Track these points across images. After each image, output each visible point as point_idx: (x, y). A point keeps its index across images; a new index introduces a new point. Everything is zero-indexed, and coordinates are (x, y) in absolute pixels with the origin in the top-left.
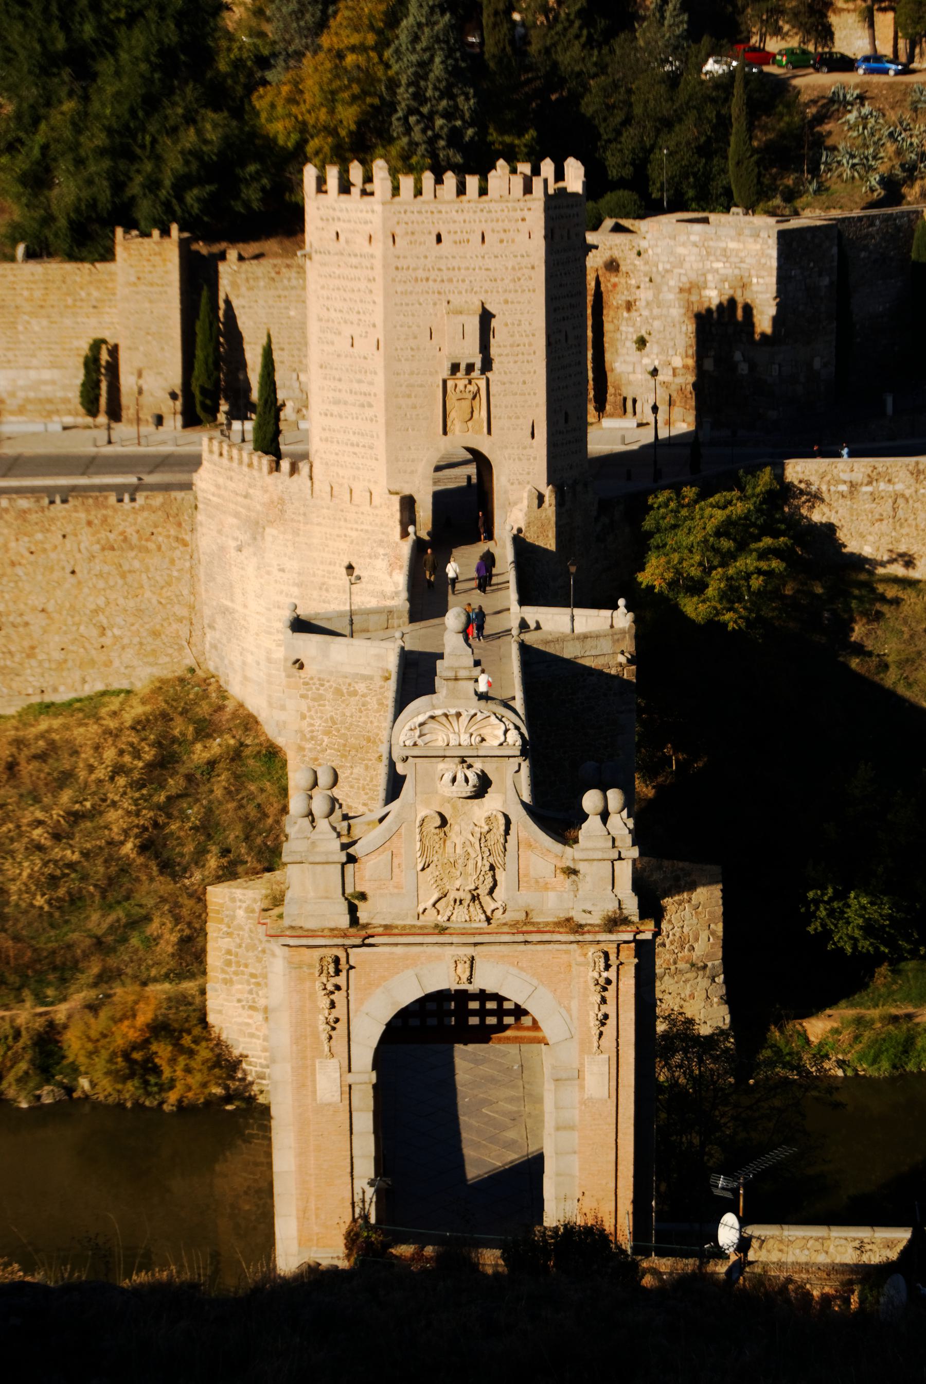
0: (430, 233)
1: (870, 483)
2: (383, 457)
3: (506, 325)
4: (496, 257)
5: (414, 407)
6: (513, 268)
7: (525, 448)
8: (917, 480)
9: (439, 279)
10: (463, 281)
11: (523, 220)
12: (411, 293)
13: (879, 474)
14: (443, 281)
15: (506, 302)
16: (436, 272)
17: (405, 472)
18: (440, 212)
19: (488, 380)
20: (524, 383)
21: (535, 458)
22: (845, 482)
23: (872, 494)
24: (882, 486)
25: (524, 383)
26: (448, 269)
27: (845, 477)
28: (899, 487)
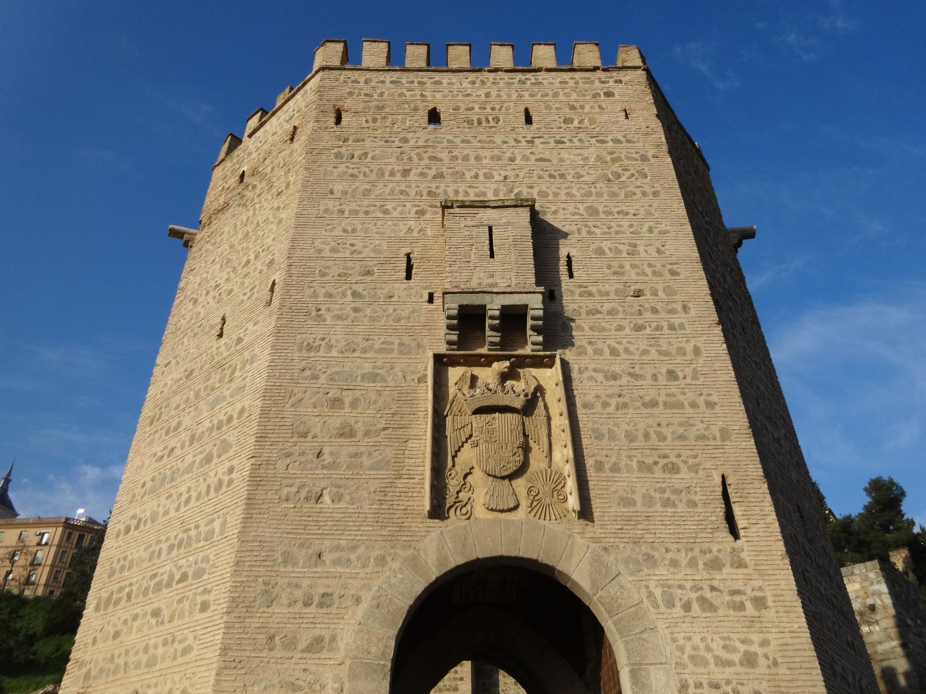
0: (416, 109)
2: (220, 596)
3: (600, 252)
5: (347, 432)
6: (599, 158)
7: (715, 565)
9: (432, 172)
10: (489, 176)
11: (608, 94)
12: (366, 193)
14: (440, 176)
15: (593, 212)
16: (426, 161)
17: (290, 644)
18: (439, 83)
19: (565, 365)
21: (760, 603)
25: (672, 375)
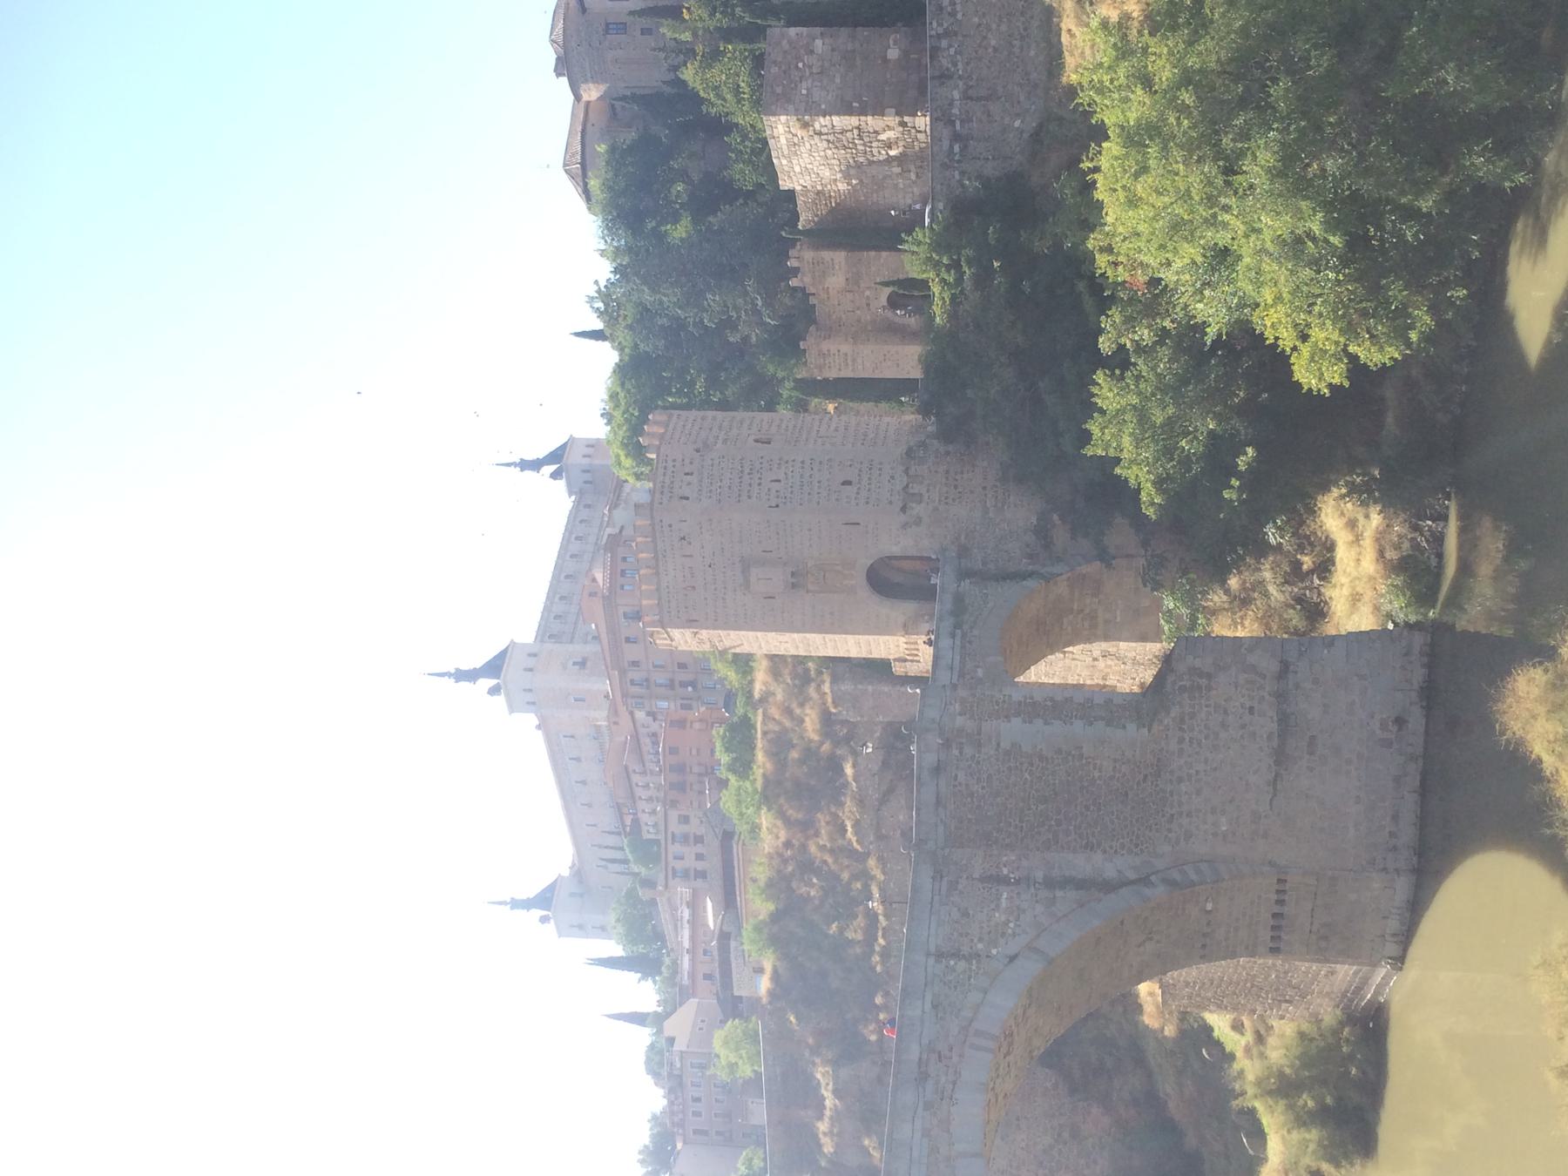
1: (952, 123)
3: (760, 542)
4: (703, 547)
5: (832, 613)
6: (712, 535)
7: (867, 532)
8: (950, 77)
9: (723, 590)
11: (670, 526)
13: (943, 115)
14: (725, 588)
18: (668, 587)
20: (810, 530)
22: (951, 147)
23: (962, 121)
24: (955, 111)
26: (715, 583)
27: (946, 144)
28: (956, 95)
